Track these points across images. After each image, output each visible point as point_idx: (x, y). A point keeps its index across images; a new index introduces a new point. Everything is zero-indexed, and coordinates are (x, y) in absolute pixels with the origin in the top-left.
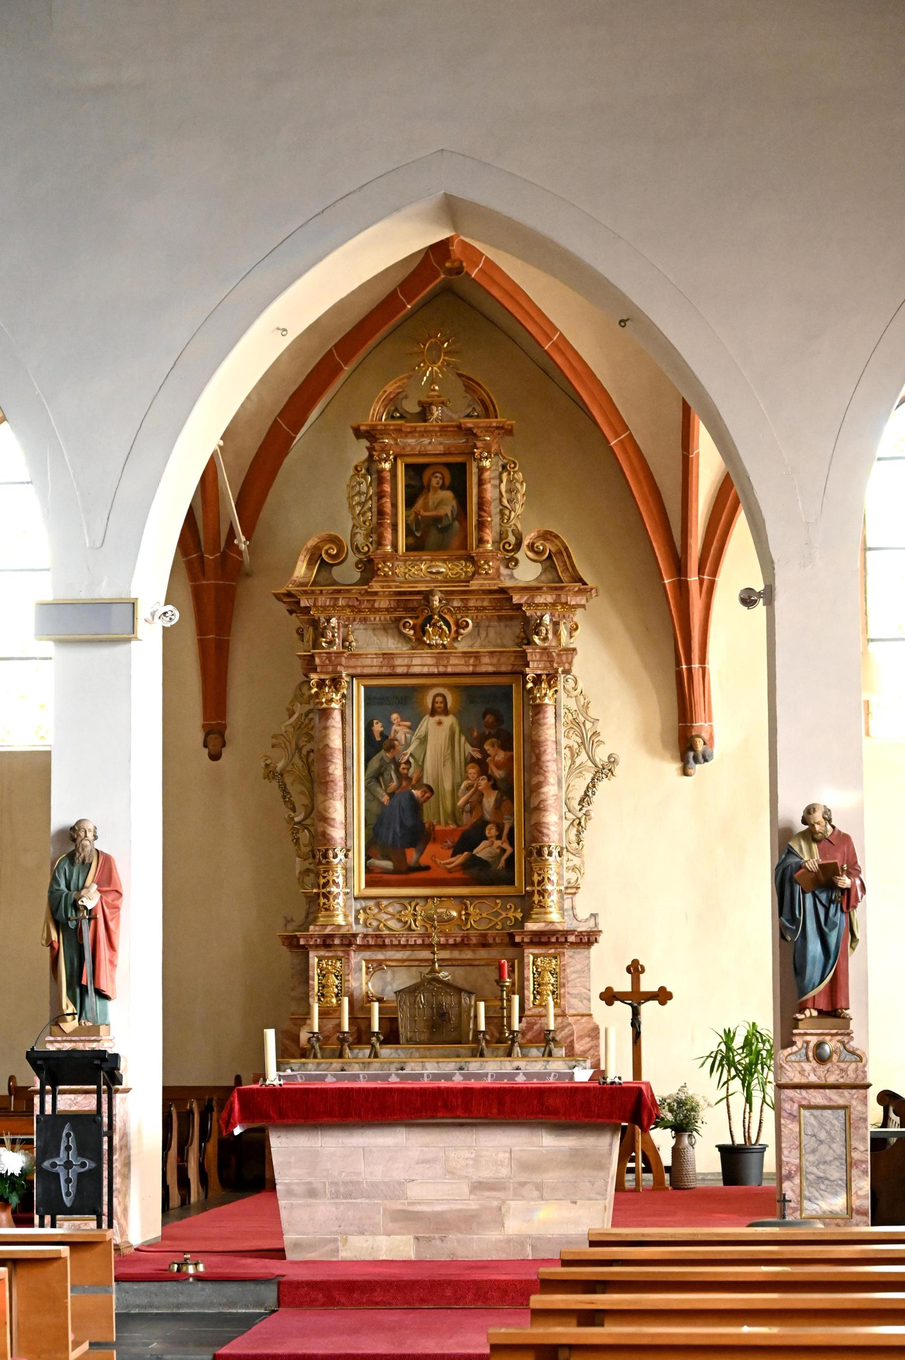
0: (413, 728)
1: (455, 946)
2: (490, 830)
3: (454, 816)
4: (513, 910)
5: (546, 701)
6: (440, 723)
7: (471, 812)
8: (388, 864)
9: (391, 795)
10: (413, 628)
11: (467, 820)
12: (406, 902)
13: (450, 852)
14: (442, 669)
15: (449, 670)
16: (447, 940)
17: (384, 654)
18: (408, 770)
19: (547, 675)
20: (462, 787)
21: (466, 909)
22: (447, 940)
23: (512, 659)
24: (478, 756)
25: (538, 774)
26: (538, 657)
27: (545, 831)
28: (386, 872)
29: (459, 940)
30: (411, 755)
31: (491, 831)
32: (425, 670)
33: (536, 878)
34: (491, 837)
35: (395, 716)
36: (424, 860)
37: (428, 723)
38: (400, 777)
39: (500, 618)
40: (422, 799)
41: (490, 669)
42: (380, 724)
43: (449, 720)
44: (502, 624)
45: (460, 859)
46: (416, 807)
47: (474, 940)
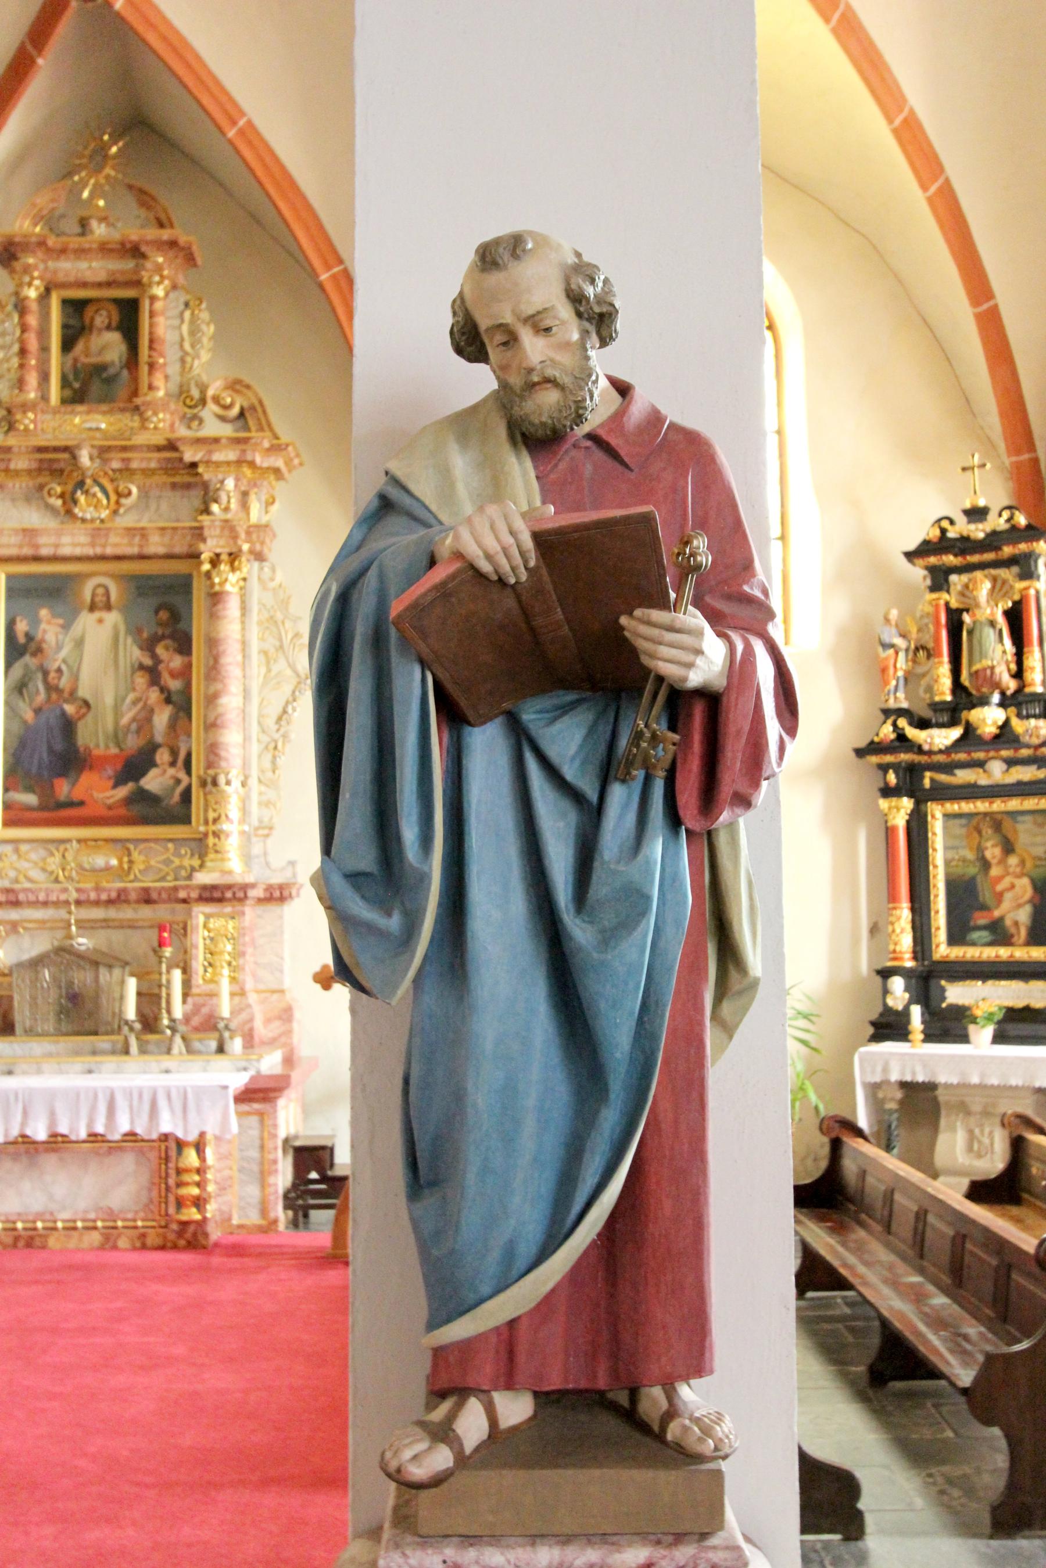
0: (66, 627)
1: (110, 902)
2: (162, 754)
3: (117, 738)
4: (189, 856)
5: (228, 587)
6: (100, 621)
7: (138, 731)
8: (31, 799)
9: (38, 711)
10: (62, 496)
11: (133, 743)
12: (52, 847)
13: (111, 783)
14: (99, 551)
15: (109, 551)
16: (99, 895)
17: (24, 530)
18: (59, 678)
19: (230, 554)
20: (128, 700)
21: (129, 855)
22: (99, 895)
23: (189, 538)
24: (148, 662)
25: (215, 680)
27: (223, 754)
28: (29, 808)
29: (114, 895)
30: (64, 661)
31: (163, 756)
32: (78, 551)
33: (211, 815)
35: (44, 613)
36: (78, 794)
37: (86, 621)
38: (50, 688)
39: (174, 486)
40: (77, 717)
41: (161, 550)
42: (25, 622)
43: (113, 618)
44: (178, 493)
45: (123, 792)
46: (68, 726)
47: (133, 896)
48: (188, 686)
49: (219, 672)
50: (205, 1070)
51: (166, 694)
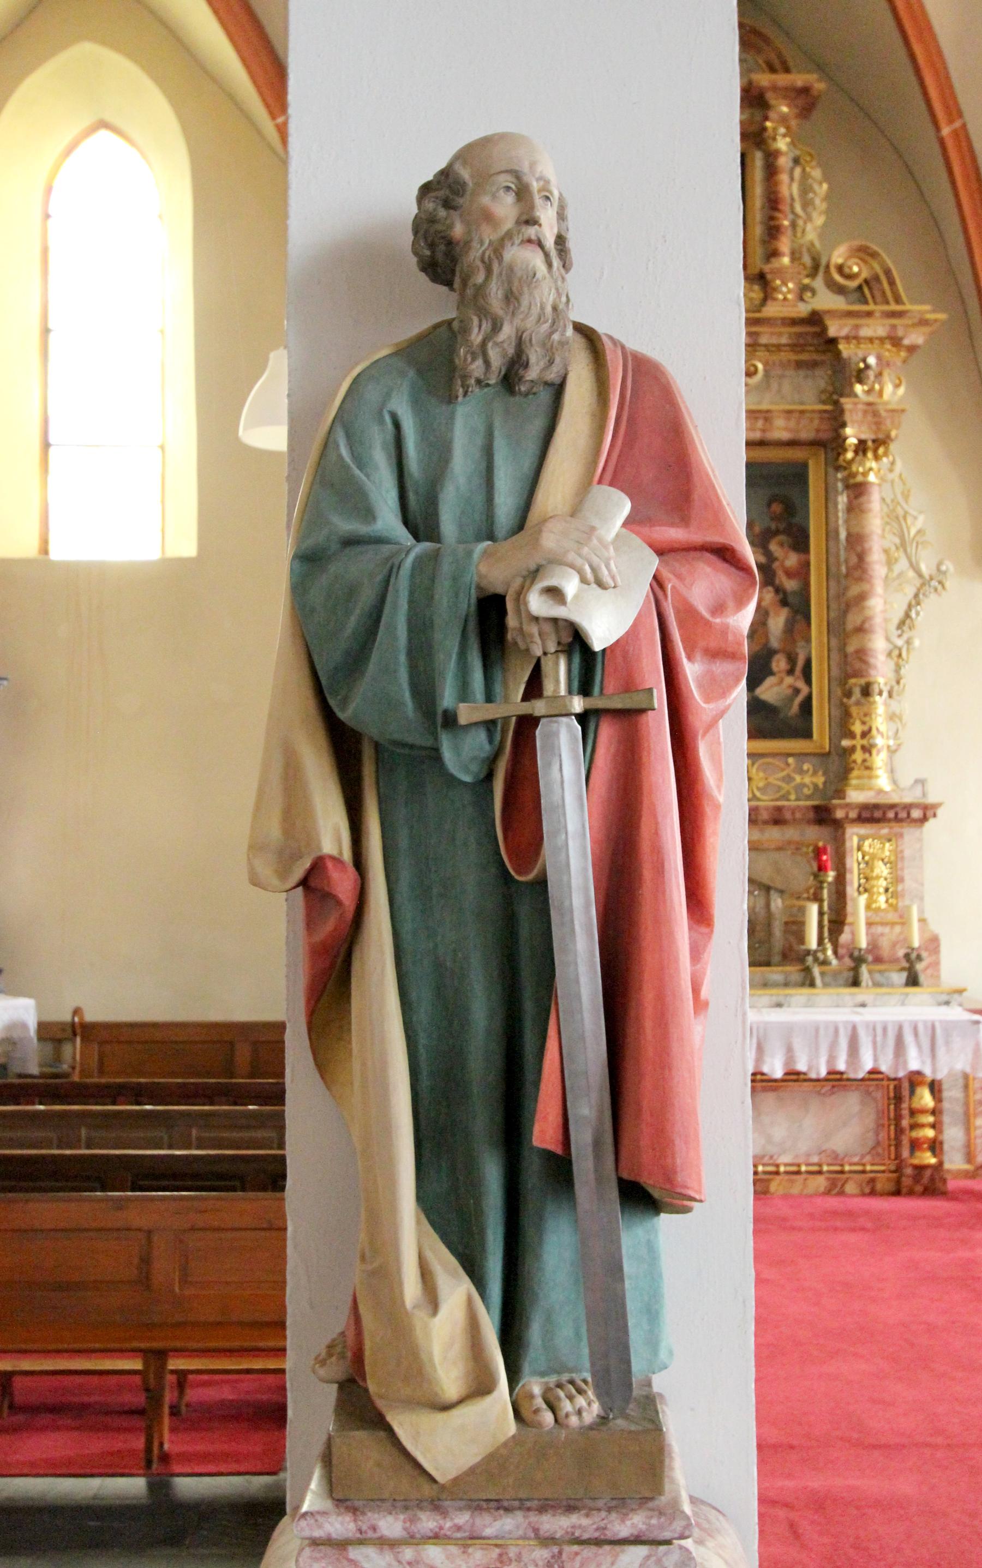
19: (874, 441)
23: (816, 422)
26: (860, 414)
27: (872, 661)
31: (779, 663)
33: (857, 728)
34: (779, 672)
39: (799, 365)
41: (785, 436)
48: (806, 585)
49: (864, 571)
50: (903, 1004)
51: (781, 596)
